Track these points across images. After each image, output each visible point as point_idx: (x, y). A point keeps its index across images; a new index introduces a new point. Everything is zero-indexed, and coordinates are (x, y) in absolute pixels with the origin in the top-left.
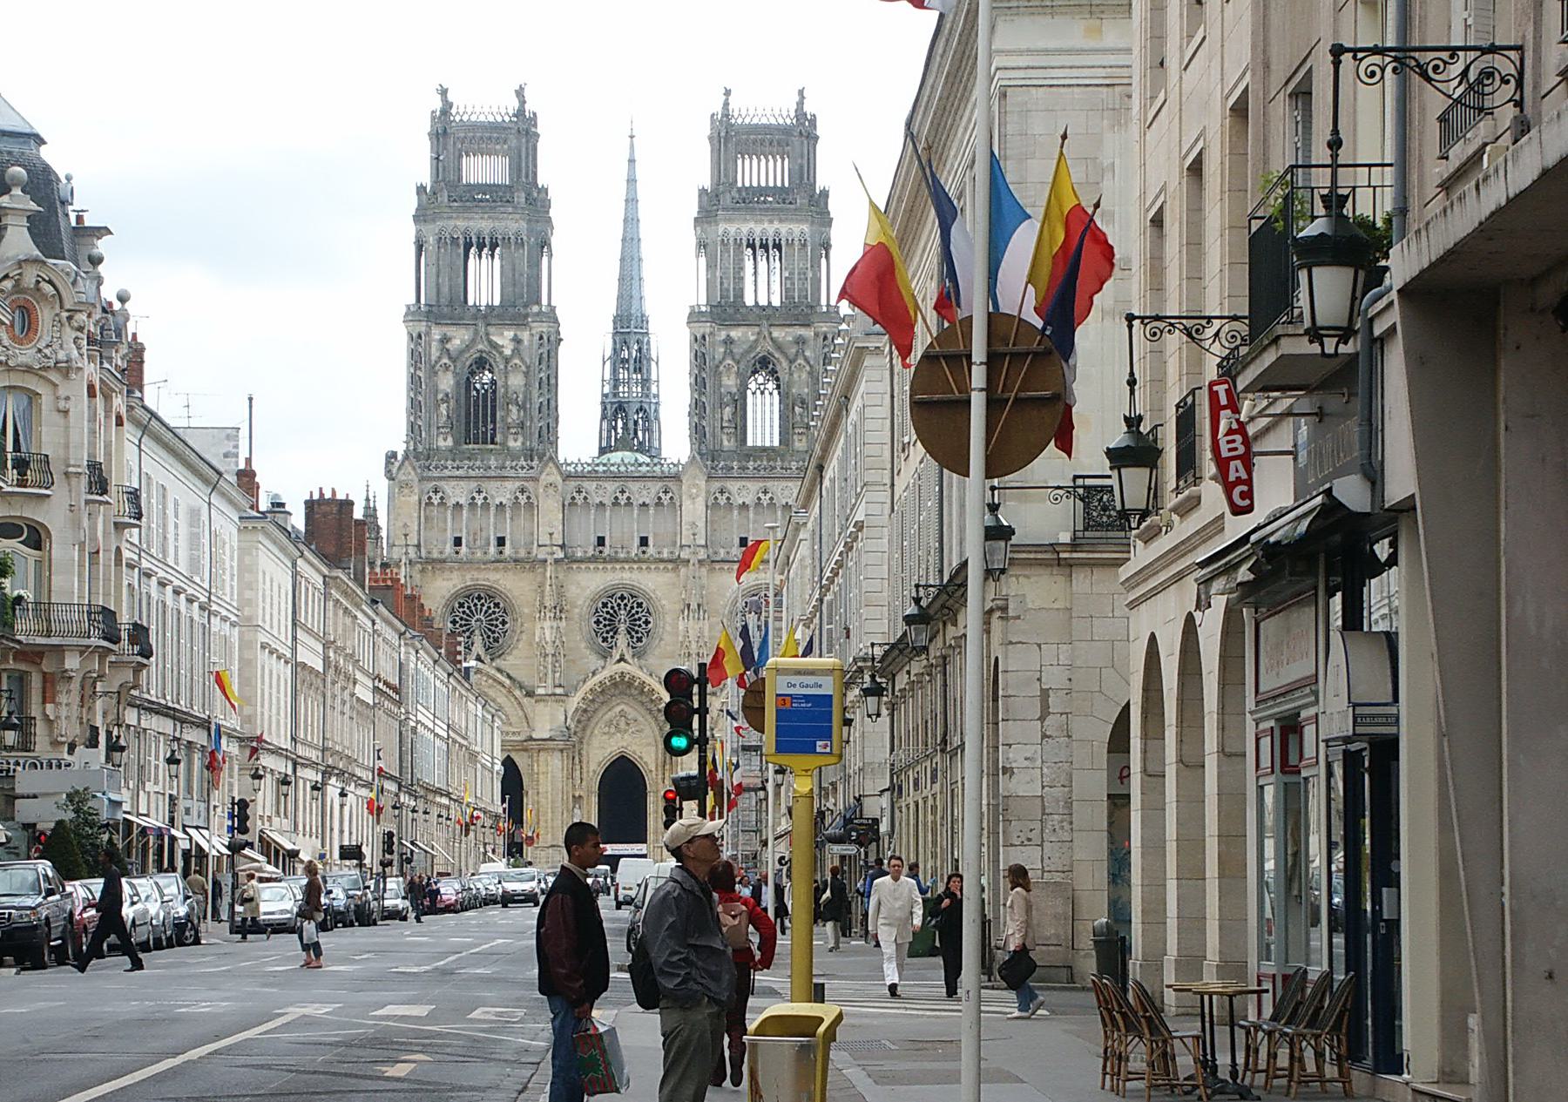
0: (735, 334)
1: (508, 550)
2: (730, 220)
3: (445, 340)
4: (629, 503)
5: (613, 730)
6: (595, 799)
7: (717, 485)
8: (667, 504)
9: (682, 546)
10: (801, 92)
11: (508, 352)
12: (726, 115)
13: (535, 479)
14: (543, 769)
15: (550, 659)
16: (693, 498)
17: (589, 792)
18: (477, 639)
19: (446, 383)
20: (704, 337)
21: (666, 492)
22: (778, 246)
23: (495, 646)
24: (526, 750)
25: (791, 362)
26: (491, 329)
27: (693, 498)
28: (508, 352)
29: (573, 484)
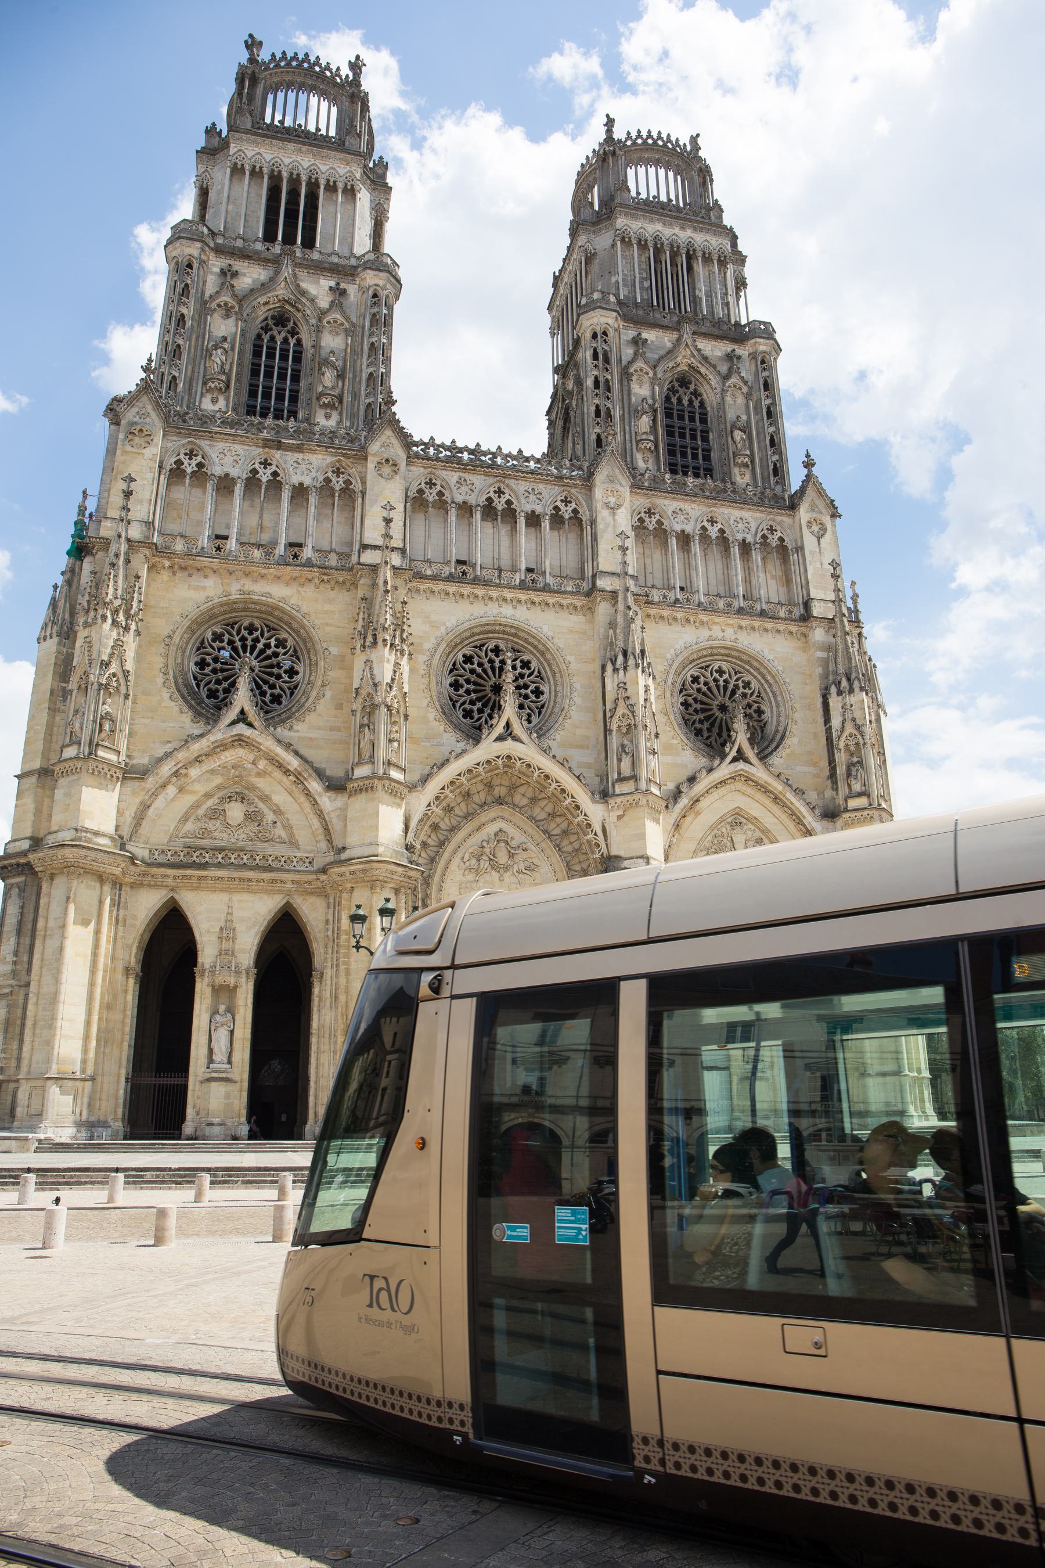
0: (650, 335)
2: (634, 217)
3: (228, 274)
4: (510, 513)
5: (484, 864)
10: (694, 140)
12: (609, 139)
13: (362, 455)
20: (605, 333)
24: (321, 892)
25: (726, 377)
26: (302, 274)
27: (613, 509)
28: (324, 303)
29: (418, 473)
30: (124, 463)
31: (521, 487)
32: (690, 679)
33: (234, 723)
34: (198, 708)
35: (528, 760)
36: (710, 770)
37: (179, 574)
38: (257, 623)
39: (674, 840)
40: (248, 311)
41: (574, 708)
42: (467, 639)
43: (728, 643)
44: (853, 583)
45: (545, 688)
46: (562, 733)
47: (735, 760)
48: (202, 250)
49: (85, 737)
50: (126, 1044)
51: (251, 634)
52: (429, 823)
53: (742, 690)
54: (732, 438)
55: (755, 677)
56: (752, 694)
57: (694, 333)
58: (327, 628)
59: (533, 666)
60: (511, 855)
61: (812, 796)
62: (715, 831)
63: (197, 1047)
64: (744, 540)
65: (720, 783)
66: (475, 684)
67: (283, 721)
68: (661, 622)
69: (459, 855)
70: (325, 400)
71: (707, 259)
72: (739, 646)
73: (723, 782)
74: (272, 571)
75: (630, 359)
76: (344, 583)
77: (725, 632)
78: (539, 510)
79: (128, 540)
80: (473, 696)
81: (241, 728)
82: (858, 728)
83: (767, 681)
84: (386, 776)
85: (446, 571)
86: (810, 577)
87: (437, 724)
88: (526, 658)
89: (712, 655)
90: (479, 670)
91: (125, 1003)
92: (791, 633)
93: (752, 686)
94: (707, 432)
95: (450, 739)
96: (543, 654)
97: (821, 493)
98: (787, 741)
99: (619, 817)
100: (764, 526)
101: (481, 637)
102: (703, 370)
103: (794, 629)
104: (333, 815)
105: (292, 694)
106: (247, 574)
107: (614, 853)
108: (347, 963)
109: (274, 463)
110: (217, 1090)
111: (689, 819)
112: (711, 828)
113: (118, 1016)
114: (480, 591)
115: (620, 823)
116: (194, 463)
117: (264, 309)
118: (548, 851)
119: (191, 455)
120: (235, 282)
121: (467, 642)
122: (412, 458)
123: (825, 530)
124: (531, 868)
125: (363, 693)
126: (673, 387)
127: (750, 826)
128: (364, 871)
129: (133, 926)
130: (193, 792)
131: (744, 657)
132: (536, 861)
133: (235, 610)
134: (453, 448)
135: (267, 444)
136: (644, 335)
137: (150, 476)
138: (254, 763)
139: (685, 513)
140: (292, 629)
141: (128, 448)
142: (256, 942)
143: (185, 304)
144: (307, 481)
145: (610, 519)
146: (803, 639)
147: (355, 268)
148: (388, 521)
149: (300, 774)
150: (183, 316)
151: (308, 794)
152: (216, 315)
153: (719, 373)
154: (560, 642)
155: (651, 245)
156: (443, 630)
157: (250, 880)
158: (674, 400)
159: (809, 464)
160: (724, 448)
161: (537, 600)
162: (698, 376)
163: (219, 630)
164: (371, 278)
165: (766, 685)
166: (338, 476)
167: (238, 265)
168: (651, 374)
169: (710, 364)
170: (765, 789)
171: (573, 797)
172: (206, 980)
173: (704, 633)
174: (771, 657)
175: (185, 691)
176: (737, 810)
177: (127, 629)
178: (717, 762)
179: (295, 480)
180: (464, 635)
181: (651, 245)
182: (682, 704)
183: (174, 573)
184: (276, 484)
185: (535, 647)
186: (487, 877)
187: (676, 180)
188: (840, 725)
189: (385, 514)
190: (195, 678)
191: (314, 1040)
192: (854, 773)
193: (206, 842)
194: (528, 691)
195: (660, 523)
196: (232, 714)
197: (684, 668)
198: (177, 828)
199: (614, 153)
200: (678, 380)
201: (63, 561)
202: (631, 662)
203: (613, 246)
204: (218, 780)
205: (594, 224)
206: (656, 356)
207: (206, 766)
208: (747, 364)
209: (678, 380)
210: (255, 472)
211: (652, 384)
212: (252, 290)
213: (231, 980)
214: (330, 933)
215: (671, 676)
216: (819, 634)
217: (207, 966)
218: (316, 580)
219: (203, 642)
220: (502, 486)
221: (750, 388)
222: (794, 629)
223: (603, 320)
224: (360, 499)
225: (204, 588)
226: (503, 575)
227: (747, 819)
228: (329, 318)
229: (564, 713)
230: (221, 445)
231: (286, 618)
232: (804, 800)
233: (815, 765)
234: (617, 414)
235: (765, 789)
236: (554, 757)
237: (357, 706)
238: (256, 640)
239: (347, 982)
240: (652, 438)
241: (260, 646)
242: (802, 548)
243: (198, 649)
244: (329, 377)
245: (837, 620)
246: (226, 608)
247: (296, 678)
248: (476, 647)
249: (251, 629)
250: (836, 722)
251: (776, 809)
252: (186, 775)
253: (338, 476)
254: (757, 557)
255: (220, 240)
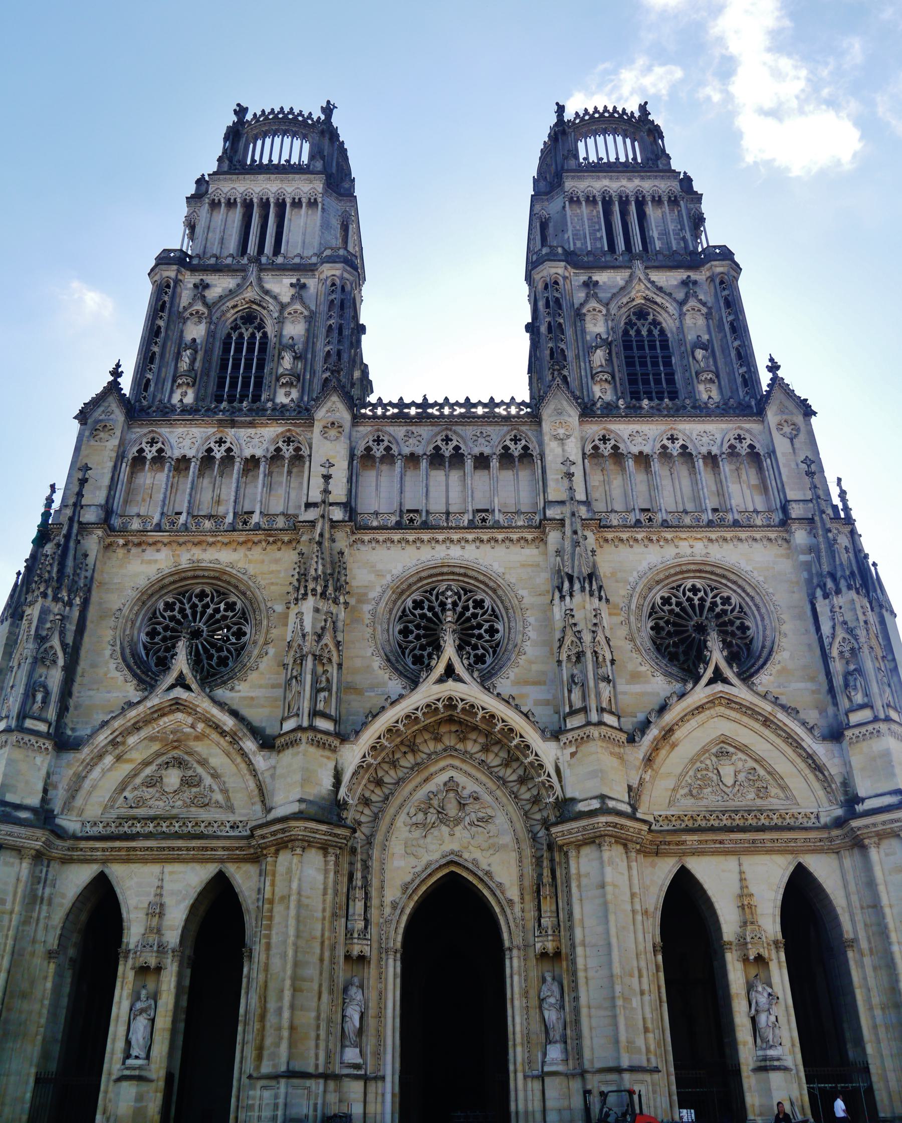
0: (601, 277)
1: (255, 518)
4: (457, 458)
5: (432, 817)
6: (393, 968)
7: (594, 429)
8: (520, 457)
9: (548, 503)
11: (285, 299)
14: (280, 891)
15: (309, 663)
16: (561, 441)
17: (383, 951)
18: (182, 648)
19: (195, 331)
20: (556, 283)
21: (515, 440)
22: (641, 205)
23: (217, 665)
24: (256, 858)
25: (682, 304)
27: (561, 441)
29: (365, 432)
30: (87, 456)
31: (469, 431)
32: (660, 602)
33: (172, 687)
34: (143, 676)
35: (471, 700)
36: (682, 696)
37: (134, 550)
38: (208, 590)
39: (647, 777)
40: (218, 314)
41: (528, 643)
42: (415, 583)
43: (698, 558)
44: (839, 480)
45: (499, 626)
46: (516, 670)
47: (711, 682)
48: (178, 271)
49: (14, 712)
50: (40, 1038)
51: (200, 601)
52: (367, 776)
53: (720, 607)
54: (694, 358)
55: (735, 591)
56: (732, 611)
57: (646, 268)
58: (272, 588)
59: (486, 605)
60: (462, 806)
61: (812, 716)
62: (698, 764)
63: (114, 1040)
64: (709, 453)
65: (697, 709)
66: (425, 628)
67: (224, 683)
68: (621, 546)
69: (406, 811)
70: (283, 380)
71: (657, 201)
72: (711, 559)
73: (700, 709)
74: (219, 538)
75: (582, 301)
76: (290, 542)
77: (693, 548)
78: (487, 451)
79: (80, 523)
80: (423, 641)
81: (179, 692)
82: (850, 631)
83: (748, 594)
84: (312, 728)
85: (394, 519)
86: (784, 478)
87: (382, 672)
88: (478, 597)
89: (682, 572)
90: (430, 614)
91: (45, 990)
92: (770, 540)
93: (733, 601)
94: (670, 357)
95: (395, 685)
96: (494, 591)
97: (789, 393)
98: (776, 657)
99: (573, 755)
100: (731, 435)
101: (430, 580)
102: (659, 300)
103: (773, 536)
104: (267, 774)
105: (238, 655)
106: (195, 544)
107: (569, 795)
108: (268, 937)
109: (228, 440)
110: (129, 1090)
111: (663, 752)
112: (693, 761)
113: (37, 1006)
114: (426, 537)
115: (574, 760)
116: (154, 449)
117: (232, 312)
118: (504, 800)
119: (152, 442)
120: (207, 293)
121: (415, 588)
122: (357, 419)
123: (798, 430)
124: (486, 820)
125: (295, 645)
126: (630, 320)
127: (740, 755)
128: (283, 831)
129: (61, 905)
130: (130, 761)
131: (719, 571)
132: (490, 812)
133: (185, 579)
134: (401, 404)
135: (221, 423)
136: (595, 278)
137: (111, 464)
138: (193, 726)
139: (641, 434)
140: (240, 591)
141: (92, 443)
142: (184, 917)
143: (161, 317)
144: (259, 453)
145: (559, 450)
146: (785, 545)
147: (315, 264)
148: (327, 478)
149: (235, 734)
150: (159, 327)
151: (243, 754)
152: (189, 323)
153: (675, 300)
154: (512, 578)
155: (599, 199)
156: (389, 578)
157: (179, 849)
158: (632, 333)
159: (774, 367)
160: (686, 369)
161: (485, 537)
162: (655, 307)
163: (171, 600)
164: (330, 271)
165: (747, 599)
166: (288, 445)
167: (210, 279)
168: (604, 312)
169: (665, 293)
170: (751, 712)
171: (521, 736)
172: (130, 962)
173: (669, 552)
174: (749, 568)
175: (131, 661)
176: (722, 738)
177: (70, 604)
178: (690, 686)
179: (247, 453)
180: (411, 581)
181: (599, 199)
182: (652, 628)
183: (129, 551)
184: (229, 458)
185: (487, 585)
186: (435, 832)
187: (625, 143)
188: (831, 631)
189: (324, 471)
190: (145, 647)
191: (240, 1029)
192: (852, 683)
193: (141, 812)
194: (482, 631)
195: (615, 448)
196: (171, 679)
197: (650, 589)
198: (113, 800)
199: (564, 133)
200: (634, 314)
201: (27, 550)
202: (577, 586)
203: (564, 207)
204: (156, 747)
205: (547, 194)
206: (609, 295)
207: (143, 733)
208: (706, 287)
209: (634, 314)
210: (210, 450)
211: (606, 320)
212: (221, 297)
213: (152, 962)
214: (260, 903)
215: (635, 600)
216: (800, 536)
217: (132, 946)
218: (264, 544)
219: (154, 613)
220: (449, 433)
221: (710, 308)
222: (773, 536)
223: (553, 271)
224: (307, 463)
225: (156, 561)
226: (451, 518)
227: (735, 747)
228: (290, 309)
229: (517, 650)
230: (180, 430)
231: (233, 581)
232: (798, 721)
233: (812, 679)
234: (570, 354)
235: (751, 712)
236: (499, 695)
237: (289, 660)
238: (207, 606)
239: (268, 958)
240: (609, 369)
241: (210, 611)
242: (774, 452)
243: (150, 619)
244: (287, 362)
245: (817, 518)
246: (176, 577)
247: (244, 639)
248: (426, 592)
249: (202, 595)
250: (826, 629)
251: (767, 732)
252: (124, 743)
253: (288, 445)
254: (726, 467)
255: (195, 262)
